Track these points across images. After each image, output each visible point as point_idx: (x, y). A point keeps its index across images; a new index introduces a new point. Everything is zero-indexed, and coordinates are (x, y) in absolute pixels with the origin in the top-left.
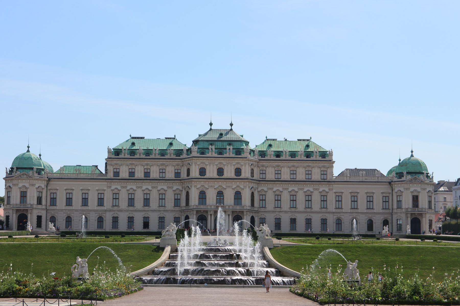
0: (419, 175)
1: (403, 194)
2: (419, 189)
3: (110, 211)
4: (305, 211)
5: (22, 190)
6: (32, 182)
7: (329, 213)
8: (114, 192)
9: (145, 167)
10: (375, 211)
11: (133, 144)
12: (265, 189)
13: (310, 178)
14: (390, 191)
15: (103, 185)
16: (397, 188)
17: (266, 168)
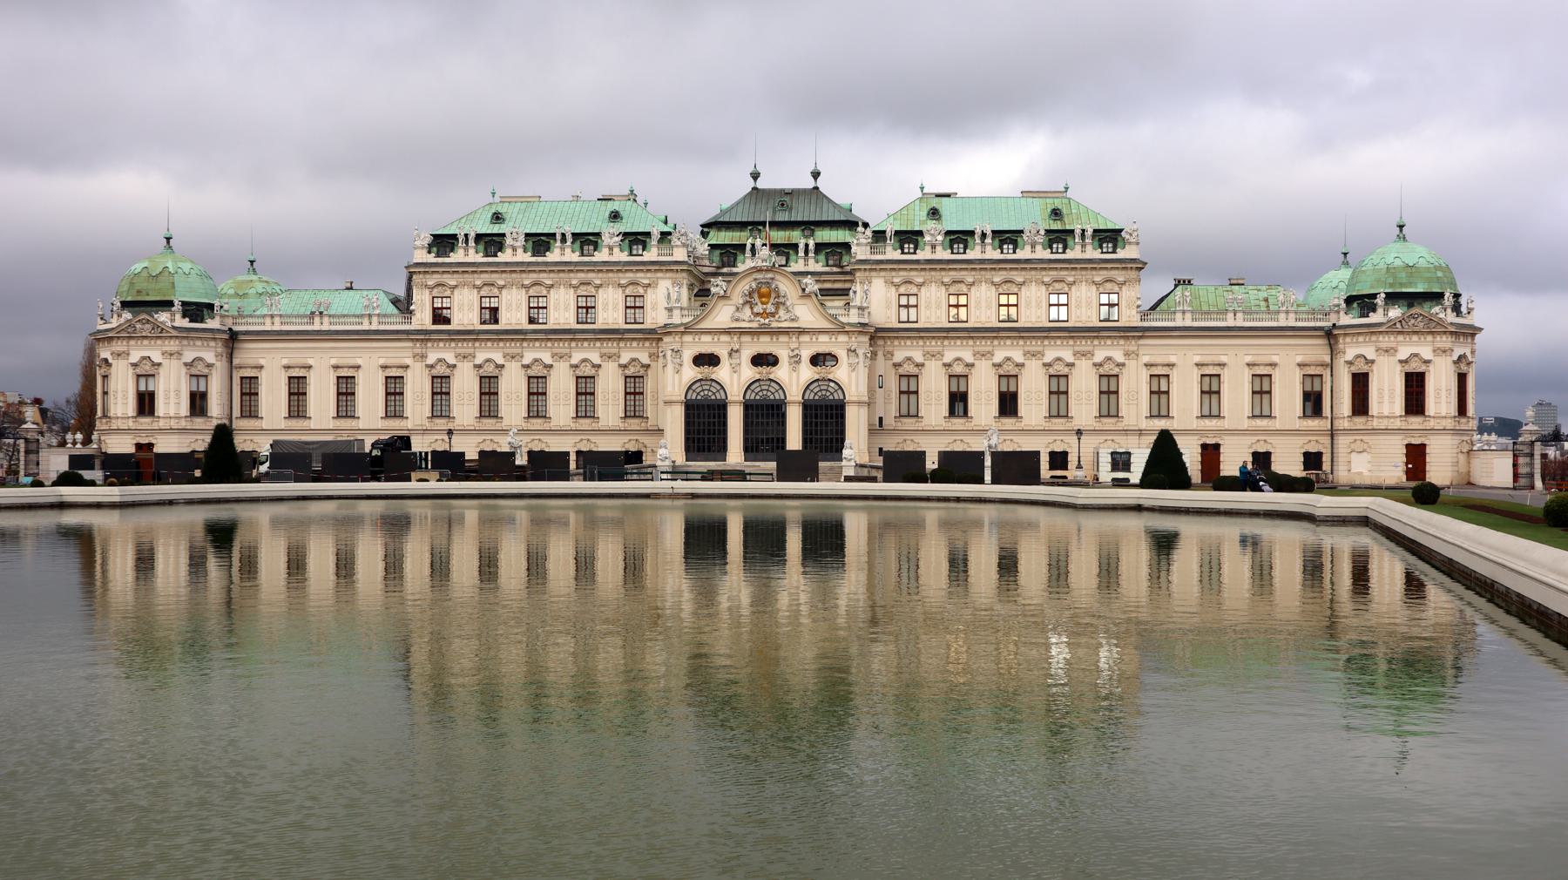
0: (1427, 305)
1: (1375, 367)
2: (1426, 353)
3: (425, 431)
4: (1048, 426)
5: (138, 371)
6: (172, 346)
7: (1126, 432)
8: (434, 372)
9: (532, 292)
10: (1277, 424)
11: (497, 218)
12: (919, 358)
13: (1063, 317)
14: (1327, 359)
15: (400, 353)
16: (1351, 349)
17: (920, 286)
